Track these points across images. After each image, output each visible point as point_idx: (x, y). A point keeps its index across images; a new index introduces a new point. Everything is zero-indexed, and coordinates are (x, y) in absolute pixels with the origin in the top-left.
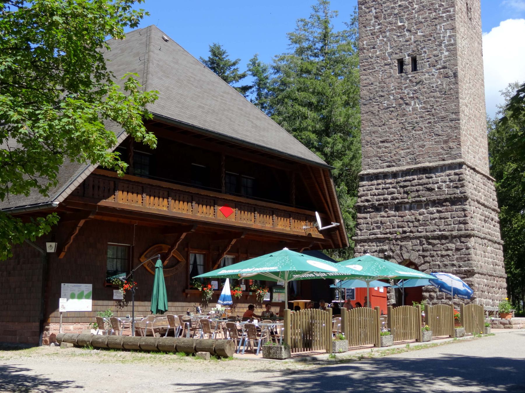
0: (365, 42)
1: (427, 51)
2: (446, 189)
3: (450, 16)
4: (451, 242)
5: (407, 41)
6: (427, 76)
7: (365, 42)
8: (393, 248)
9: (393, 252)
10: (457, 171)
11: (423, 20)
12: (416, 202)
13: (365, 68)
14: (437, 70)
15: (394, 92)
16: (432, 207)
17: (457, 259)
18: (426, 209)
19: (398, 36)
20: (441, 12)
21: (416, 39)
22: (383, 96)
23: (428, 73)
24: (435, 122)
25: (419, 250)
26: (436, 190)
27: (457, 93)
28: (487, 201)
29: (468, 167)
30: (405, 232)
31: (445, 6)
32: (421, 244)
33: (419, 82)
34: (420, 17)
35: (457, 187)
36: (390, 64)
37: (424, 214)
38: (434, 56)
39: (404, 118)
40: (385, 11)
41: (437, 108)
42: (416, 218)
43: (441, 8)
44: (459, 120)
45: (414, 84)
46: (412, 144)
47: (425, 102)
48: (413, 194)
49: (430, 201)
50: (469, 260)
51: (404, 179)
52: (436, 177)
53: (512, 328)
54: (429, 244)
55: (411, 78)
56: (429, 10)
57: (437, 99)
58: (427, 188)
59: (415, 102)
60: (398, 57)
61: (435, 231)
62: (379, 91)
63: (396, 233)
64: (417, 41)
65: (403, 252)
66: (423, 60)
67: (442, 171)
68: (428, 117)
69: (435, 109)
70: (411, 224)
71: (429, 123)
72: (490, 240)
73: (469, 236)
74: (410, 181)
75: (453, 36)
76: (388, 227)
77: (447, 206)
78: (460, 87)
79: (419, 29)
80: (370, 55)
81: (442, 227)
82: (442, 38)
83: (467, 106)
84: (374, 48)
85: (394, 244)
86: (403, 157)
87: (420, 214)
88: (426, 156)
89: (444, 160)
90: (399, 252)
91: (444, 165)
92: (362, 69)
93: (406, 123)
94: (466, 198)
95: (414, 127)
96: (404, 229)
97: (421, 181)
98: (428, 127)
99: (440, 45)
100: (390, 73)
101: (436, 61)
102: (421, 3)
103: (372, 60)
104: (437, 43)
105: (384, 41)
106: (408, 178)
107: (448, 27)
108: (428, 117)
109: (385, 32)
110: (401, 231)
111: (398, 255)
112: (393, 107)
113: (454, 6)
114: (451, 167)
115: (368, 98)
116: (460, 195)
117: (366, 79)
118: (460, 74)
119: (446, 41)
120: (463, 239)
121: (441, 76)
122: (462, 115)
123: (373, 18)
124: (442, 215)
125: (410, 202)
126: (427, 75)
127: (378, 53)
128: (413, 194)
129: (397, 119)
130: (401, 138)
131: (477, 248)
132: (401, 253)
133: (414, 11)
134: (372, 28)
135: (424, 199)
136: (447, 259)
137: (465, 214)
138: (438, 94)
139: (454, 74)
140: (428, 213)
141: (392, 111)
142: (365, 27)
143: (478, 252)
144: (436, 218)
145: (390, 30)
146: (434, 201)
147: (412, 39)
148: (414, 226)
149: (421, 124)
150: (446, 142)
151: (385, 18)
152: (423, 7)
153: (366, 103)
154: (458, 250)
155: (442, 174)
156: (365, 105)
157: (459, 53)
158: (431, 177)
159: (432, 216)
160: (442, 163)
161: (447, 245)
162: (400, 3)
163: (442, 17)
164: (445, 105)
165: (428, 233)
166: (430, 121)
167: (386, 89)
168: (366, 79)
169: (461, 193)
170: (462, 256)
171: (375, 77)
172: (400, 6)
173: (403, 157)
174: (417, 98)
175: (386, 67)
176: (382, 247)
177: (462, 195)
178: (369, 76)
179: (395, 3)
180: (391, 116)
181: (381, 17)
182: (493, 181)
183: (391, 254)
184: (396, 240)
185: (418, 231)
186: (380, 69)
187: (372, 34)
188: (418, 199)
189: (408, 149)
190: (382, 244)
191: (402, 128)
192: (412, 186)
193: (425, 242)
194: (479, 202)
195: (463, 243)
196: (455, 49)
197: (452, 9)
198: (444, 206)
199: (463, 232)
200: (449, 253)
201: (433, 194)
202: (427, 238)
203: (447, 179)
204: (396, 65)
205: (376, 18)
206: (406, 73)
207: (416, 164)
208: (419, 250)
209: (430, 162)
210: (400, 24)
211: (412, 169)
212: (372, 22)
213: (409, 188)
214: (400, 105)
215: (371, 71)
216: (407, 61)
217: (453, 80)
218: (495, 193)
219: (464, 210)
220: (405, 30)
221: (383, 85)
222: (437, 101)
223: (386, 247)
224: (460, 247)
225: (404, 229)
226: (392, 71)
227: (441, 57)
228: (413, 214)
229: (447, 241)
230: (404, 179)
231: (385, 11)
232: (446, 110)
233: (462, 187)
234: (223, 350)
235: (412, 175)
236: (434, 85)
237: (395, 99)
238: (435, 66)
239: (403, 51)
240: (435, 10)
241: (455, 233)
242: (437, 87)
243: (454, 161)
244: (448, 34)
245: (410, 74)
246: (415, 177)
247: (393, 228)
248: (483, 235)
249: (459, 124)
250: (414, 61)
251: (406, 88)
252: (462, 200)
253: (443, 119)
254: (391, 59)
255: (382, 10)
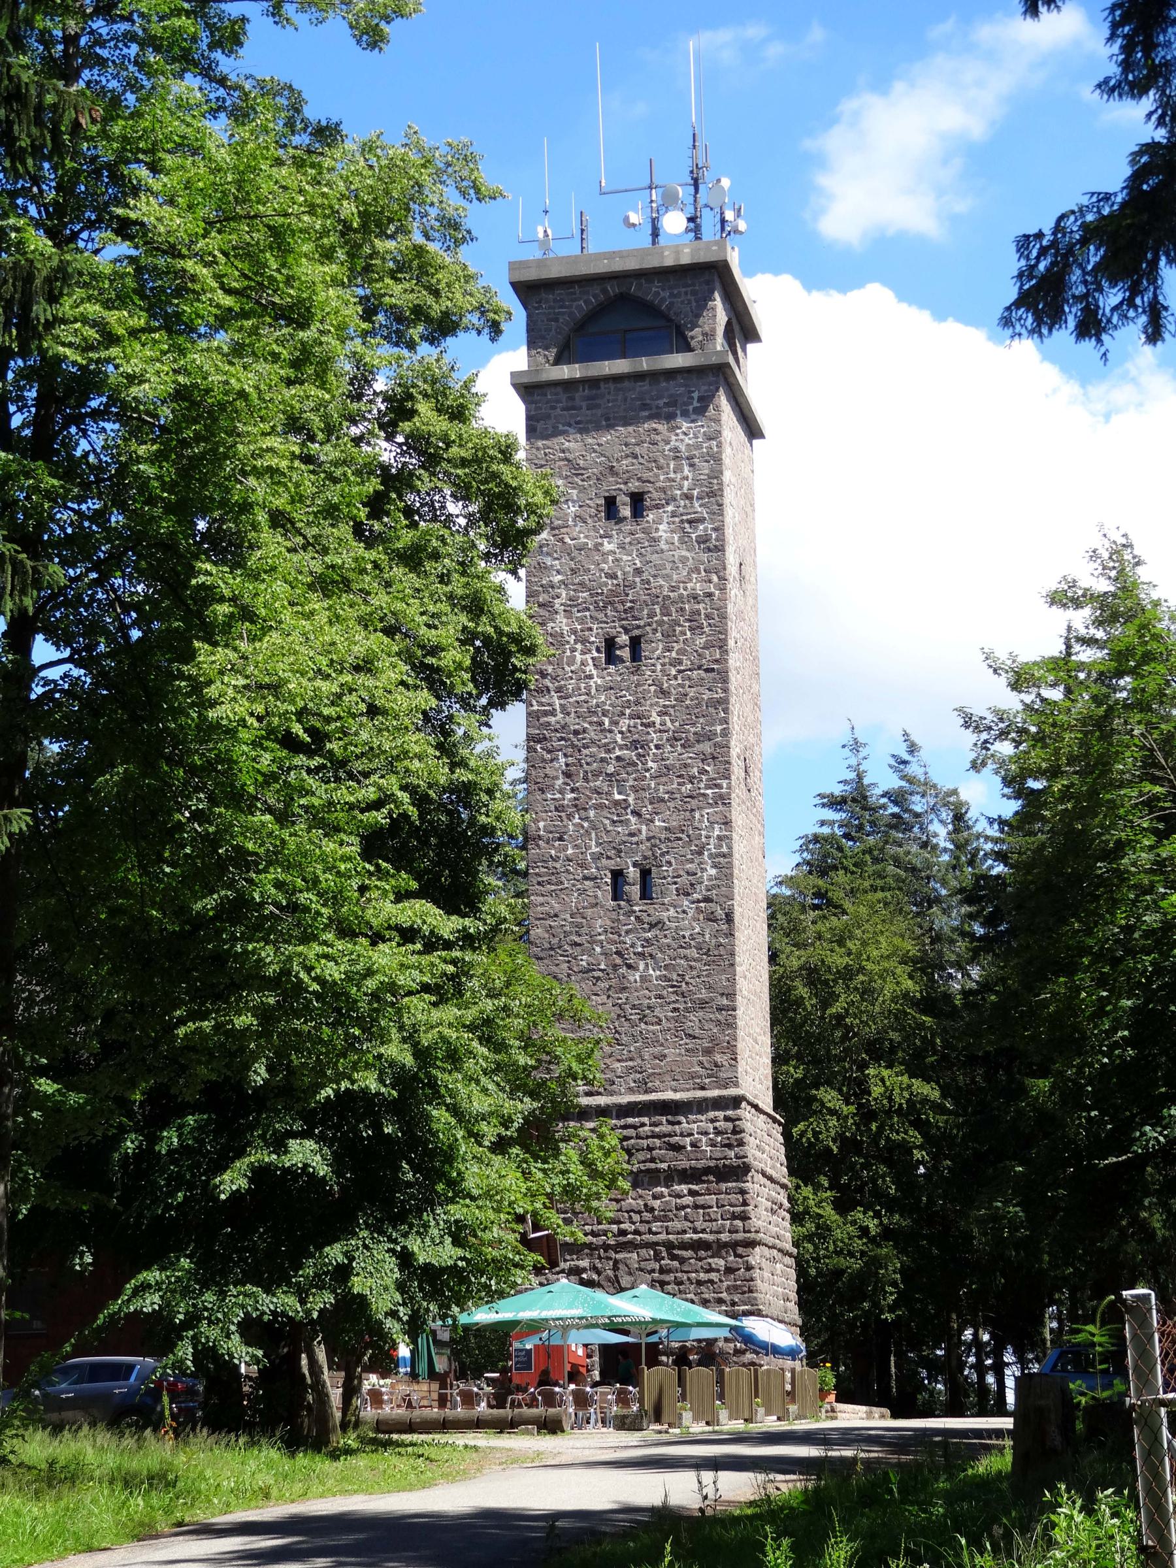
0: (541, 824)
1: (673, 861)
2: (708, 1149)
3: (721, 797)
4: (716, 1255)
5: (632, 835)
6: (672, 912)
7: (541, 824)
8: (599, 1265)
9: (599, 1273)
10: (729, 1113)
11: (666, 796)
12: (648, 1171)
13: (540, 879)
14: (693, 903)
15: (603, 937)
16: (680, 1184)
17: (728, 1288)
18: (667, 1187)
19: (614, 822)
20: (702, 785)
21: (651, 834)
22: (580, 945)
23: (675, 907)
24: (687, 1010)
25: (653, 1271)
26: (689, 1148)
27: (733, 954)
28: (773, 1167)
29: (749, 1103)
30: (623, 1233)
31: (712, 775)
32: (658, 1257)
33: (656, 924)
34: (661, 787)
35: (729, 1146)
36: (596, 878)
37: (662, 1196)
38: (688, 873)
39: (624, 996)
40: (588, 764)
41: (692, 981)
42: (646, 1205)
43: (704, 778)
44: (734, 1010)
45: (645, 926)
46: (639, 1051)
47: (666, 967)
48: (641, 1156)
49: (676, 1170)
50: (751, 1291)
51: (622, 1122)
52: (688, 1123)
53: (836, 1418)
54: (673, 1257)
55: (638, 914)
56: (678, 777)
57: (693, 963)
58: (669, 1144)
59: (647, 965)
60: (611, 864)
61: (685, 1232)
62: (571, 932)
63: (605, 1235)
64: (654, 837)
65: (620, 1273)
66: (665, 878)
67: (700, 1112)
68: (673, 998)
69: (687, 983)
70: (636, 1217)
71: (675, 1010)
72: (780, 1250)
73: (752, 1244)
74: (635, 1127)
75: (727, 837)
76: (589, 1221)
77: (709, 1182)
78: (737, 942)
79: (657, 814)
80: (553, 852)
81: (699, 1225)
82: (704, 840)
83: (745, 977)
84: (561, 839)
85: (600, 1258)
86: (620, 1077)
87: (655, 1197)
88: (667, 1078)
89: (703, 1088)
90: (610, 1273)
91: (705, 1099)
92: (535, 882)
93: (627, 1006)
94: (746, 1168)
95: (645, 1016)
96: (622, 1226)
97: (657, 1129)
98: (673, 1017)
99: (700, 853)
100: (596, 897)
101: (692, 885)
102: (663, 759)
103: (558, 865)
104: (693, 848)
105: (583, 827)
106: (630, 1120)
107: (717, 818)
108: (673, 998)
109: (585, 809)
110: (616, 1231)
111: (609, 1279)
112: (600, 970)
113: (728, 778)
114: (719, 1104)
115: (547, 946)
116: (735, 1162)
117: (542, 904)
118: (737, 917)
119: (712, 846)
120: (740, 1250)
121: (701, 918)
122: (740, 1001)
123: (561, 776)
124: (701, 1200)
125: (635, 1170)
126: (672, 909)
127: (570, 851)
128: (641, 1156)
129: (609, 997)
130: (617, 1036)
131: (763, 1265)
132: (616, 1276)
133: (647, 774)
134: (558, 796)
135: (664, 1166)
136: (708, 1288)
137: (744, 1200)
138: (694, 953)
139: (727, 915)
140: (670, 1195)
141: (598, 979)
142: (542, 791)
143: (766, 1275)
144: (688, 1206)
145: (597, 807)
146: (685, 1170)
147: (644, 833)
148: (641, 1222)
149: (657, 1012)
150: (708, 1052)
151: (586, 780)
152: (666, 767)
153: (541, 955)
154: (729, 1270)
155: (699, 1117)
156: (541, 959)
157: (736, 871)
158: (679, 1123)
159: (678, 1201)
160: (700, 1094)
161: (710, 1260)
162: (618, 753)
163: (704, 795)
164: (707, 976)
165: (670, 1236)
166: (677, 1006)
167: (584, 930)
168: (542, 904)
169: (737, 1157)
170: (739, 1283)
171: (563, 902)
172: (618, 758)
173: (620, 1077)
174: (651, 955)
175: (587, 883)
176: (576, 1263)
177: (740, 1161)
178: (549, 899)
179: (609, 751)
180: (594, 988)
181: (578, 774)
182: (780, 1124)
183: (595, 1277)
184: (606, 1247)
185: (650, 1232)
186: (574, 885)
187: (557, 809)
188: (653, 1166)
189: (631, 1059)
190: (575, 1257)
191: (619, 1016)
192: (638, 1137)
193: (664, 1254)
194: (764, 1174)
195: (741, 1257)
196: (730, 866)
197: (724, 783)
198: (704, 1182)
199: (740, 1236)
200: (714, 1276)
201: (682, 1157)
202: (669, 1246)
203: (710, 1127)
204: (609, 881)
205: (568, 775)
206: (628, 901)
207: (646, 1092)
208: (653, 1271)
209: (675, 1091)
210: (618, 797)
211: (640, 1103)
212: (560, 782)
213: (633, 1141)
214: (615, 967)
215: (553, 887)
216: (631, 875)
217: (725, 927)
218: (783, 1150)
219: (743, 1192)
220: (629, 811)
221: (580, 920)
222: (691, 967)
223: (584, 1263)
224: (734, 1266)
225: (622, 1226)
226: (599, 893)
227: (702, 877)
228: (641, 1197)
229: (710, 1253)
230: (622, 1122)
231: (588, 764)
232: (710, 988)
233: (738, 1145)
234: (560, 1422)
235: (640, 1116)
236: (687, 934)
237: (604, 954)
238: (688, 894)
239: (623, 854)
240: (691, 779)
241: (725, 1237)
242: (693, 939)
243: (725, 1092)
244: (717, 833)
245: (637, 904)
246: (646, 1120)
247: (599, 1223)
248: (771, 1241)
249: (735, 1017)
250: (645, 874)
251: (627, 932)
252: (740, 1171)
253: (703, 1004)
254: (597, 868)
255: (579, 760)
